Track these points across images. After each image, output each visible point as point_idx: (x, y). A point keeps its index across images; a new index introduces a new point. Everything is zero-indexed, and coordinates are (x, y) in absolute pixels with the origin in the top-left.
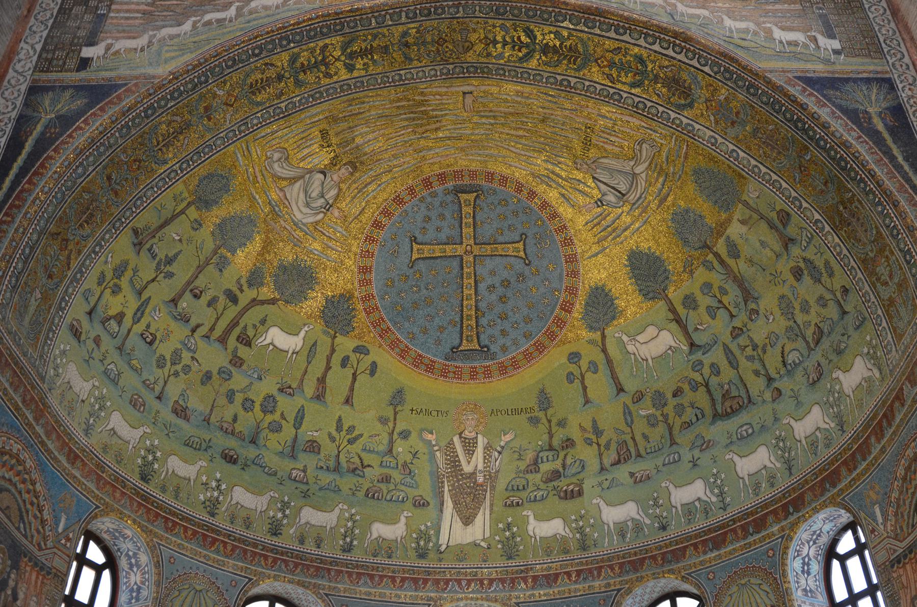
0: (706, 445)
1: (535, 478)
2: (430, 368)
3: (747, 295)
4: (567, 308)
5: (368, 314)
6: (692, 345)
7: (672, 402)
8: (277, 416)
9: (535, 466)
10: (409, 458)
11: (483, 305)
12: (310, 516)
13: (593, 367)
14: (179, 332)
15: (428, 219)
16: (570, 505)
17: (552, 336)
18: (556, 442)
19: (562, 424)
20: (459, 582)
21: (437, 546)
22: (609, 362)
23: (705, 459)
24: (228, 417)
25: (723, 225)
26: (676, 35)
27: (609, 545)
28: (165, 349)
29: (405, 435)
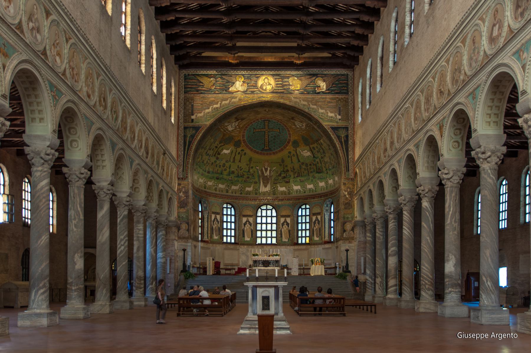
0: (315, 178)
1: (280, 178)
2: (257, 153)
3: (324, 152)
4: (289, 143)
5: (244, 143)
6: (314, 157)
7: (309, 166)
8: (225, 167)
9: (280, 175)
10: (253, 173)
11: (270, 140)
12: (234, 187)
13: (294, 155)
14: (207, 157)
15: (258, 125)
16: (287, 184)
17: (285, 147)
18: (285, 170)
19: (286, 166)
20: (264, 200)
21: (259, 192)
22: (297, 155)
23: (314, 180)
24: (216, 170)
25: (320, 140)
26: (309, 114)
27: (294, 194)
28: (205, 162)
29: (252, 168)
